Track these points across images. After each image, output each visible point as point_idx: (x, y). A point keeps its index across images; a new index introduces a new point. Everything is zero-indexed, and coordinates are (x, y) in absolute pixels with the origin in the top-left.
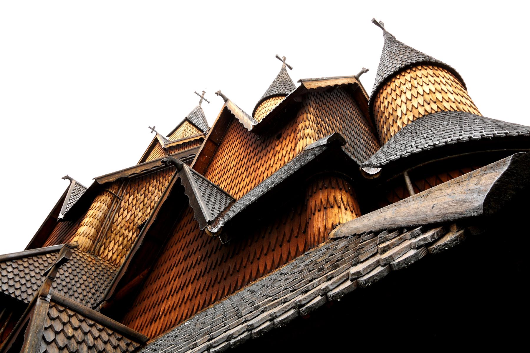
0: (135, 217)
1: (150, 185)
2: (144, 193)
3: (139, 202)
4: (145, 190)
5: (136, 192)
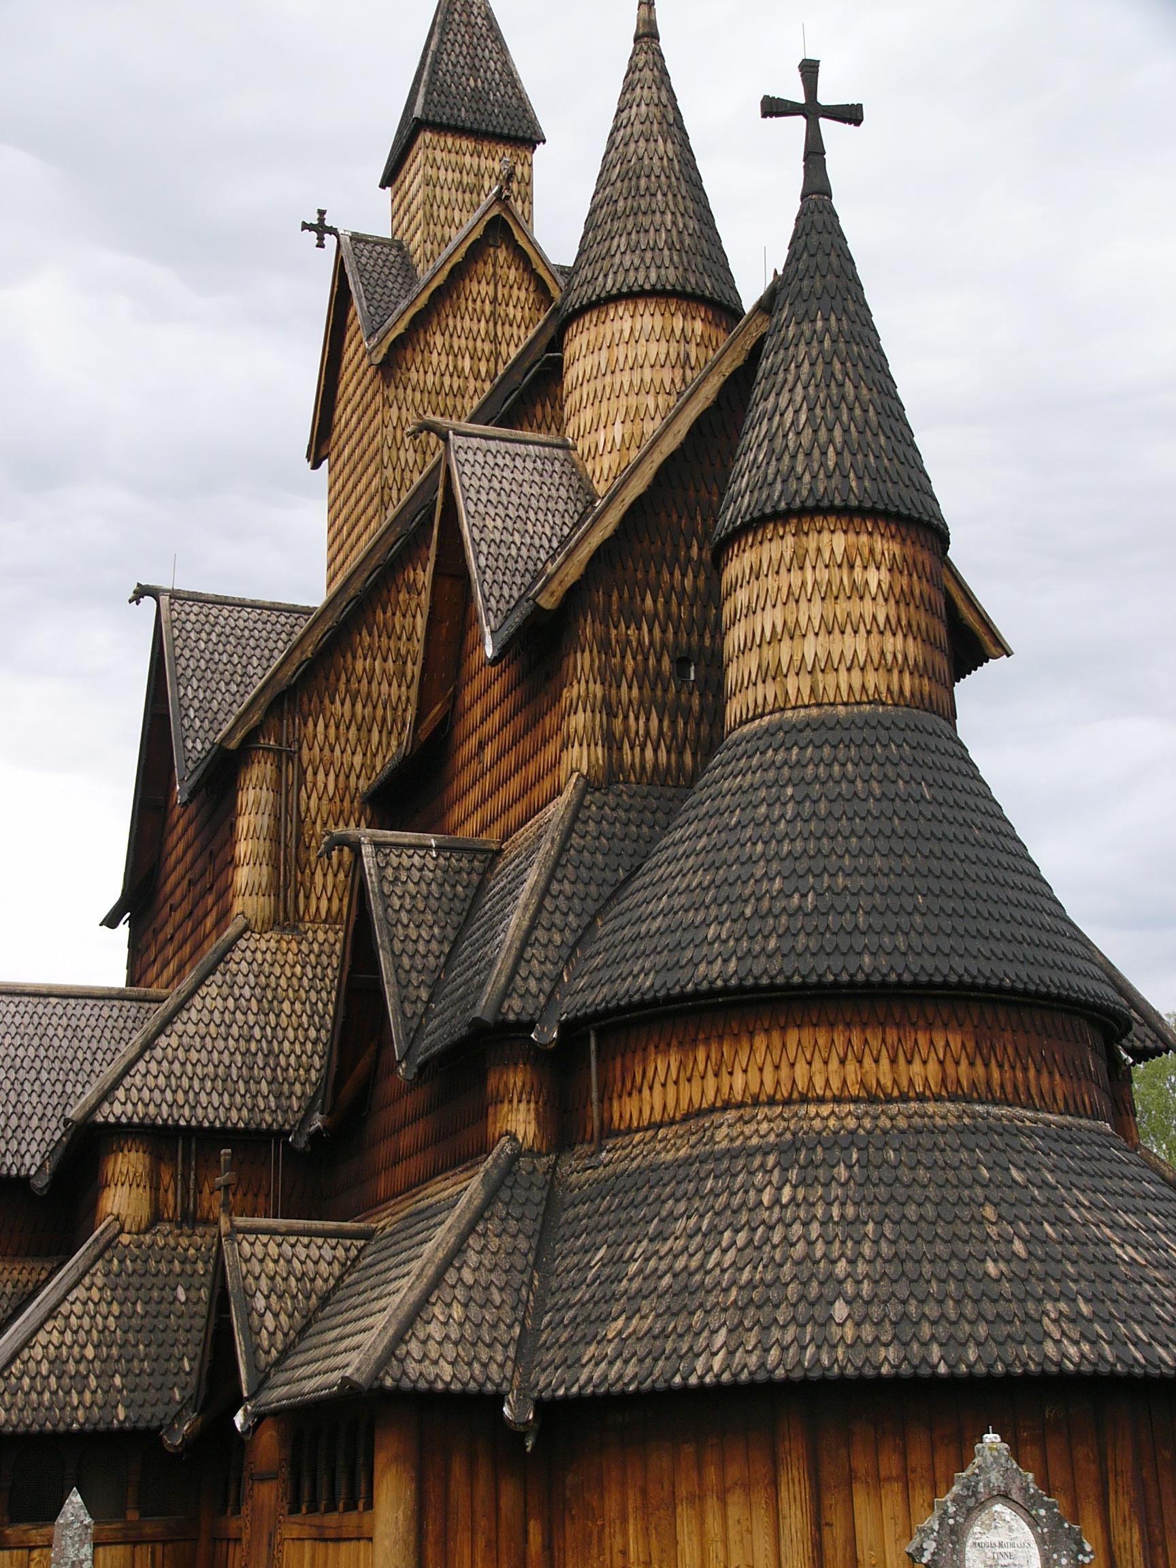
0: (348, 777)
1: (354, 658)
2: (347, 691)
3: (342, 727)
4: (348, 681)
5: (327, 701)
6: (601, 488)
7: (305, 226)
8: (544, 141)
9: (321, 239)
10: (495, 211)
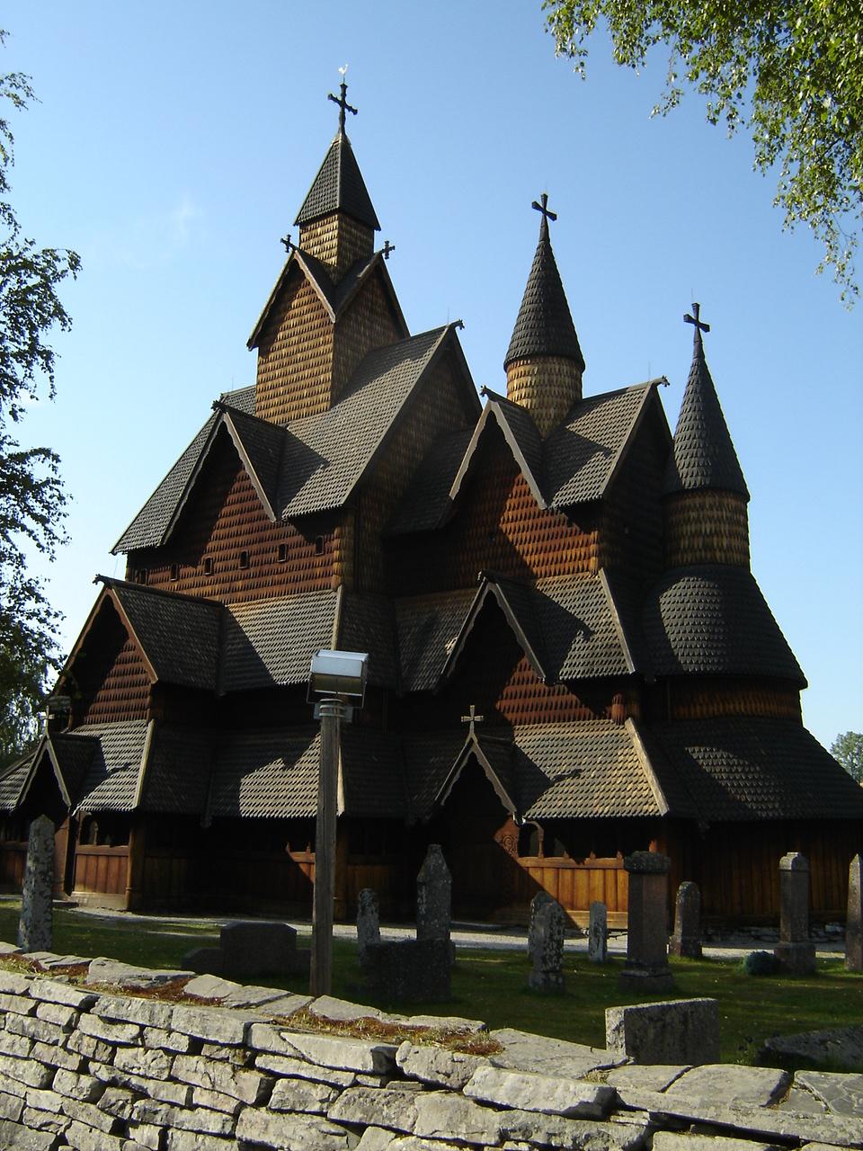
6: (544, 434)
7: (283, 241)
8: (380, 230)
9: (288, 248)
10: (378, 262)
